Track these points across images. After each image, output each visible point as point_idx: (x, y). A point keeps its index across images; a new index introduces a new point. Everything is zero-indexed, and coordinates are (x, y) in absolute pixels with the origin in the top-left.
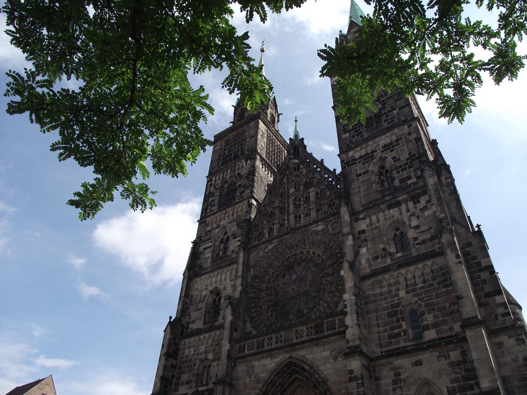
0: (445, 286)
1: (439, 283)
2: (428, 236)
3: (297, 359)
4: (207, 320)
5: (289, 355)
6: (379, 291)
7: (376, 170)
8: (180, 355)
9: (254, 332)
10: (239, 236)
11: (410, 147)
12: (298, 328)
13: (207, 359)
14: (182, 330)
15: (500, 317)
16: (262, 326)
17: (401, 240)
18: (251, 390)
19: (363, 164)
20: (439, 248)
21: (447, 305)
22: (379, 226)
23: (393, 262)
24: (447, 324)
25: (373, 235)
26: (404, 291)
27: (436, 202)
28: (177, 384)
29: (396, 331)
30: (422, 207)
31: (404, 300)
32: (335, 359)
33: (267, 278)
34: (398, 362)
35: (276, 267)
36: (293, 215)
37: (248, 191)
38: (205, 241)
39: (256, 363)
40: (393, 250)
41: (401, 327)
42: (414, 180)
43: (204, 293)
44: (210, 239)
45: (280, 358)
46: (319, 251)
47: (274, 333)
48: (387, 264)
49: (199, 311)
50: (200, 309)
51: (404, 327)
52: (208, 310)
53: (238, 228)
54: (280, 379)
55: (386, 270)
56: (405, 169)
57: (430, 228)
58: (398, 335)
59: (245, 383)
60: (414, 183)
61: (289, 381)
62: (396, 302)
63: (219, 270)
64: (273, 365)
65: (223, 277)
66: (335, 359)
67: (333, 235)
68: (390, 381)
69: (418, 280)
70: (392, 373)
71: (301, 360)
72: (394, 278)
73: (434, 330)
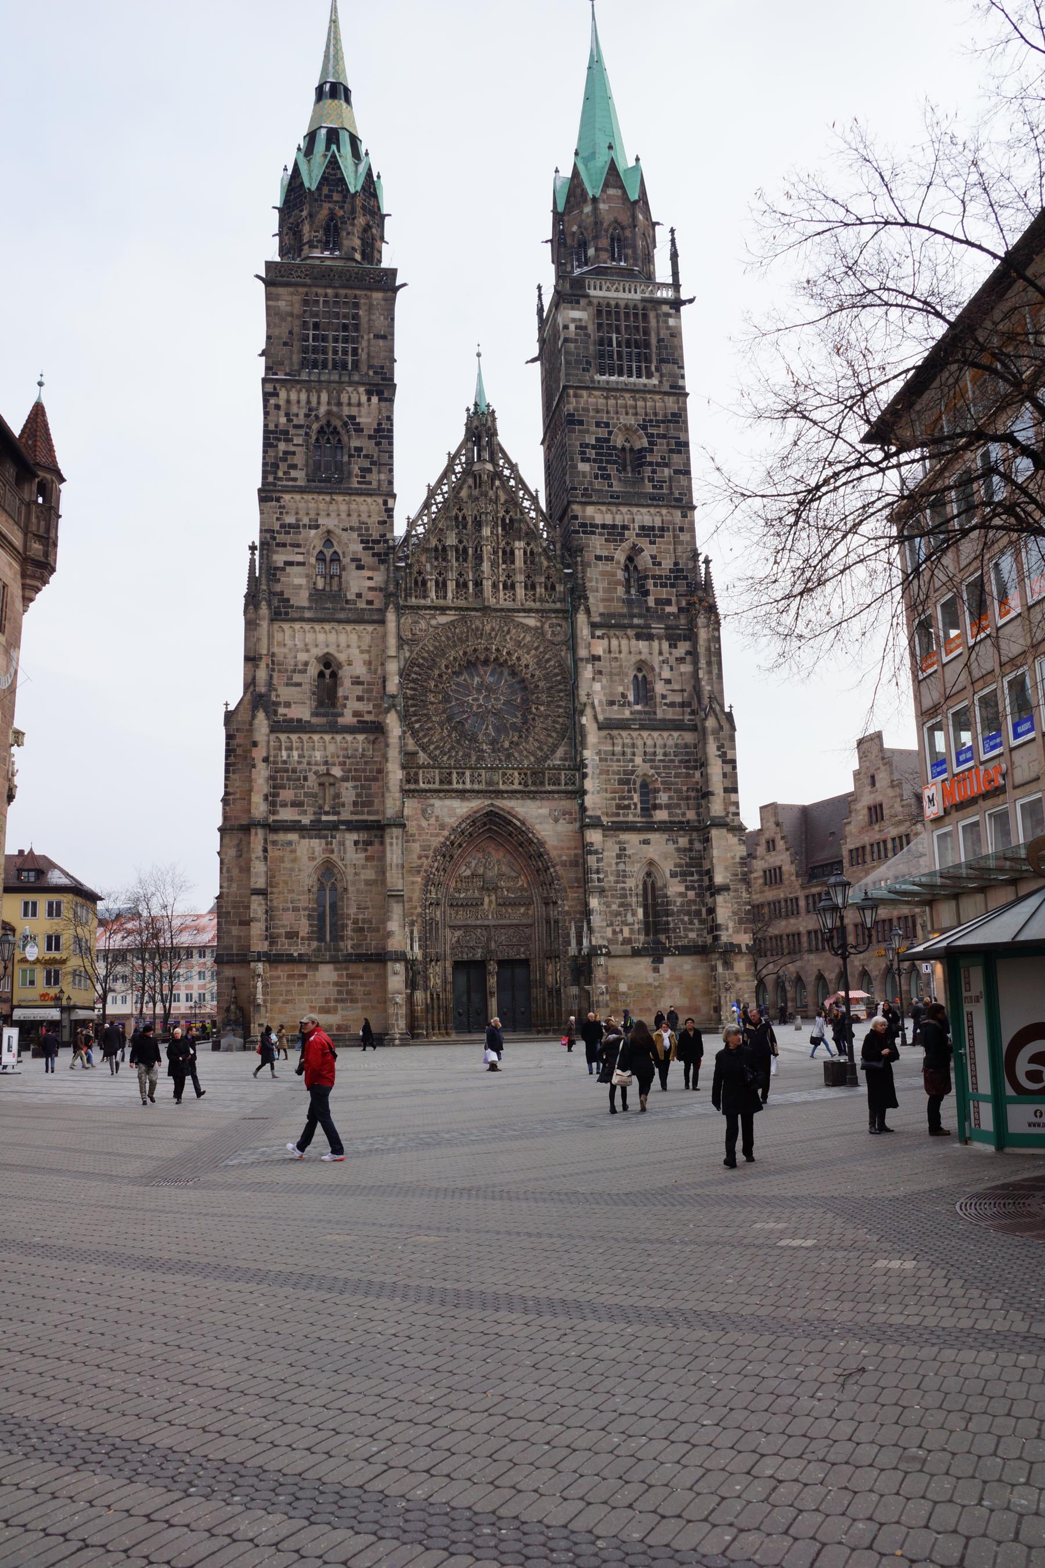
0: (686, 768)
1: (680, 761)
2: (678, 699)
5: (489, 802)
7: (622, 559)
9: (421, 754)
13: (328, 774)
16: (432, 747)
17: (643, 688)
19: (607, 540)
21: (685, 788)
29: (626, 802)
32: (556, 821)
33: (437, 672)
34: (625, 837)
36: (490, 583)
37: (383, 477)
38: (284, 545)
39: (437, 803)
40: (631, 698)
43: (302, 657)
44: (298, 546)
45: (475, 804)
46: (528, 659)
49: (298, 689)
50: (299, 685)
55: (623, 725)
57: (682, 691)
58: (628, 807)
60: (673, 614)
63: (335, 625)
66: (556, 821)
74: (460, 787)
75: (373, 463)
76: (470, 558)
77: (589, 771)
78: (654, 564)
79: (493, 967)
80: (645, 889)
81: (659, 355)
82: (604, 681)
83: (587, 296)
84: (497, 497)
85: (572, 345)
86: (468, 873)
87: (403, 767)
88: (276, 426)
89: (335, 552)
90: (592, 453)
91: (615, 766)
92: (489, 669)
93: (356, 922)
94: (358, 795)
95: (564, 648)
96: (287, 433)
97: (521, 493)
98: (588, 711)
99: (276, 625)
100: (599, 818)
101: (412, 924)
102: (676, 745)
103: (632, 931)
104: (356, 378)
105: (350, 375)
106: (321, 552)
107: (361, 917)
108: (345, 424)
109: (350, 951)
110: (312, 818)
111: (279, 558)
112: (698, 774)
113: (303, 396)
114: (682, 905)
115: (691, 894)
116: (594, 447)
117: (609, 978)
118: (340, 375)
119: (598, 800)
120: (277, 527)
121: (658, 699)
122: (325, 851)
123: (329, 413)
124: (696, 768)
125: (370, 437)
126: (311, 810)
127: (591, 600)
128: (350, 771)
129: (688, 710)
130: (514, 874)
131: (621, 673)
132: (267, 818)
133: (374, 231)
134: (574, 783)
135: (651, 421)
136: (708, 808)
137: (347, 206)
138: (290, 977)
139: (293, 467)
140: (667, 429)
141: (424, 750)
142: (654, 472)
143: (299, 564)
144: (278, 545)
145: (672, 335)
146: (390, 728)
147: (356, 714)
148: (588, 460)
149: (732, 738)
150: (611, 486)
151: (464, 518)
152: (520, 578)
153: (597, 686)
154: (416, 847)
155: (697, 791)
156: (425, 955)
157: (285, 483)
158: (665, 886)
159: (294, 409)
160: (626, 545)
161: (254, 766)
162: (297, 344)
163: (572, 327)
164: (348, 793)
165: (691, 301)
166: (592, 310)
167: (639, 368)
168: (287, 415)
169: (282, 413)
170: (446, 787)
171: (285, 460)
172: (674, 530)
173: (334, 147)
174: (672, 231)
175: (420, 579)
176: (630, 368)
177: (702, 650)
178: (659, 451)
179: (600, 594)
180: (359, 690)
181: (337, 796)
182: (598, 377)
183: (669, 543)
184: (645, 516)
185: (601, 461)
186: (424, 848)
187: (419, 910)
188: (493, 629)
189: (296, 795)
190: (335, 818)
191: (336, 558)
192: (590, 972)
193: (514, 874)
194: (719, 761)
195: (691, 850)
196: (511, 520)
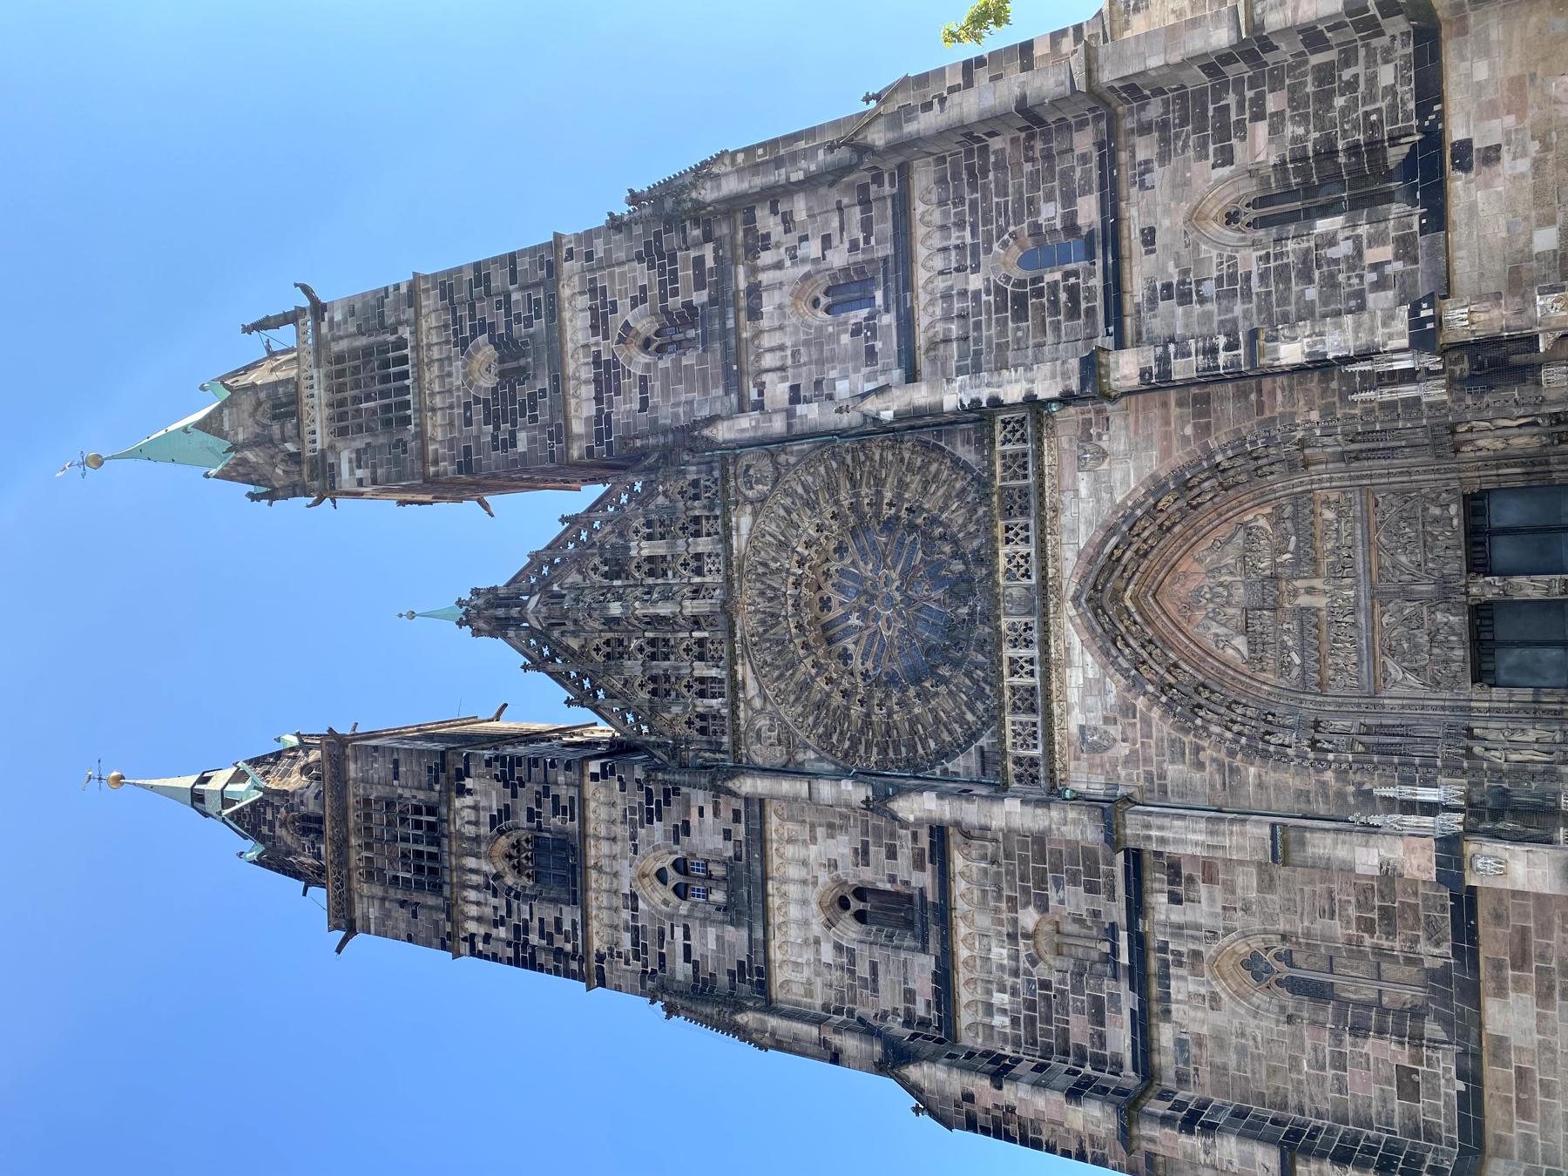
0: (985, 174)
1: (974, 189)
2: (856, 214)
3: (1084, 577)
4: (913, 944)
5: (1069, 604)
6: (955, 345)
7: (644, 359)
8: (1008, 1051)
9: (984, 741)
11: (622, 255)
12: (1002, 569)
14: (926, 1037)
16: (970, 717)
17: (845, 291)
20: (892, 185)
21: (1028, 167)
22: (794, 345)
23: (893, 307)
24: (1073, 168)
25: (810, 362)
26: (972, 277)
28: (1099, 1062)
29: (1063, 296)
30: (781, 228)
32: (1103, 455)
33: (837, 699)
35: (813, 671)
36: (687, 603)
37: (561, 779)
38: (662, 957)
39: (1075, 720)
41: (1056, 283)
42: (708, 251)
43: (828, 953)
44: (662, 933)
47: (1001, 649)
48: (894, 325)
49: (881, 969)
50: (874, 967)
51: (1058, 276)
52: (882, 939)
53: (660, 819)
54: (1132, 642)
56: (674, 272)
57: (840, 209)
58: (1073, 292)
59: (1130, 760)
60: (716, 251)
61: (1138, 619)
62: (992, 298)
64: (1089, 659)
65: (794, 872)
66: (1103, 455)
67: (776, 481)
68: (1180, 310)
69: (954, 241)
70: (1162, 305)
71: (1089, 563)
72: (932, 303)
73: (1079, 200)
74: (1037, 668)
75: (546, 789)
76: (661, 635)
77: (984, 395)
78: (644, 300)
79: (1487, 588)
80: (1262, 223)
82: (833, 374)
84: (573, 587)
85: (379, 471)
86: (1240, 642)
87: (1000, 790)
88: (509, 944)
89: (675, 865)
92: (836, 598)
93: (1367, 926)
94: (1074, 881)
95: (782, 458)
96: (517, 927)
98: (870, 406)
99: (777, 993)
101: (1366, 796)
102: (942, 203)
103: (1377, 240)
106: (676, 890)
107: (1352, 912)
108: (501, 832)
109: (1446, 949)
110: (1124, 985)
111: (681, 970)
112: (996, 143)
113: (472, 895)
114: (1305, 117)
116: (497, 428)
117: (1519, 279)
119: (1046, 368)
120: (637, 966)
121: (860, 257)
122: (1196, 972)
123: (489, 857)
124: (984, 150)
125: (514, 795)
126: (1107, 984)
127: (705, 412)
128: (1026, 890)
129: (873, 188)
130: (1241, 534)
131: (818, 340)
134: (1021, 422)
137: (277, 801)
138: (1525, 1111)
139: (558, 922)
141: (973, 736)
142: (518, 318)
143: (687, 936)
144: (662, 966)
145: (352, 314)
147: (919, 865)
148: (513, 435)
149: (922, 80)
150: (543, 391)
151: (607, 643)
153: (843, 388)
154: (1174, 771)
155: (1031, 137)
156: (1453, 770)
157: (580, 942)
158: (1251, 173)
159: (488, 911)
161: (1011, 1110)
162: (416, 897)
163: (359, 473)
164: (1071, 900)
165: (306, 290)
166: (339, 445)
168: (496, 924)
171: (550, 935)
172: (591, 270)
175: (698, 723)
177: (758, 182)
178: (492, 315)
180: (877, 853)
181: (1079, 920)
182: (411, 427)
183: (612, 276)
184: (576, 326)
185: (513, 411)
186: (1178, 754)
187: (1329, 776)
188: (762, 594)
190: (1123, 935)
191: (681, 866)
192: (1494, 342)
193: (1241, 534)
196: (605, 563)
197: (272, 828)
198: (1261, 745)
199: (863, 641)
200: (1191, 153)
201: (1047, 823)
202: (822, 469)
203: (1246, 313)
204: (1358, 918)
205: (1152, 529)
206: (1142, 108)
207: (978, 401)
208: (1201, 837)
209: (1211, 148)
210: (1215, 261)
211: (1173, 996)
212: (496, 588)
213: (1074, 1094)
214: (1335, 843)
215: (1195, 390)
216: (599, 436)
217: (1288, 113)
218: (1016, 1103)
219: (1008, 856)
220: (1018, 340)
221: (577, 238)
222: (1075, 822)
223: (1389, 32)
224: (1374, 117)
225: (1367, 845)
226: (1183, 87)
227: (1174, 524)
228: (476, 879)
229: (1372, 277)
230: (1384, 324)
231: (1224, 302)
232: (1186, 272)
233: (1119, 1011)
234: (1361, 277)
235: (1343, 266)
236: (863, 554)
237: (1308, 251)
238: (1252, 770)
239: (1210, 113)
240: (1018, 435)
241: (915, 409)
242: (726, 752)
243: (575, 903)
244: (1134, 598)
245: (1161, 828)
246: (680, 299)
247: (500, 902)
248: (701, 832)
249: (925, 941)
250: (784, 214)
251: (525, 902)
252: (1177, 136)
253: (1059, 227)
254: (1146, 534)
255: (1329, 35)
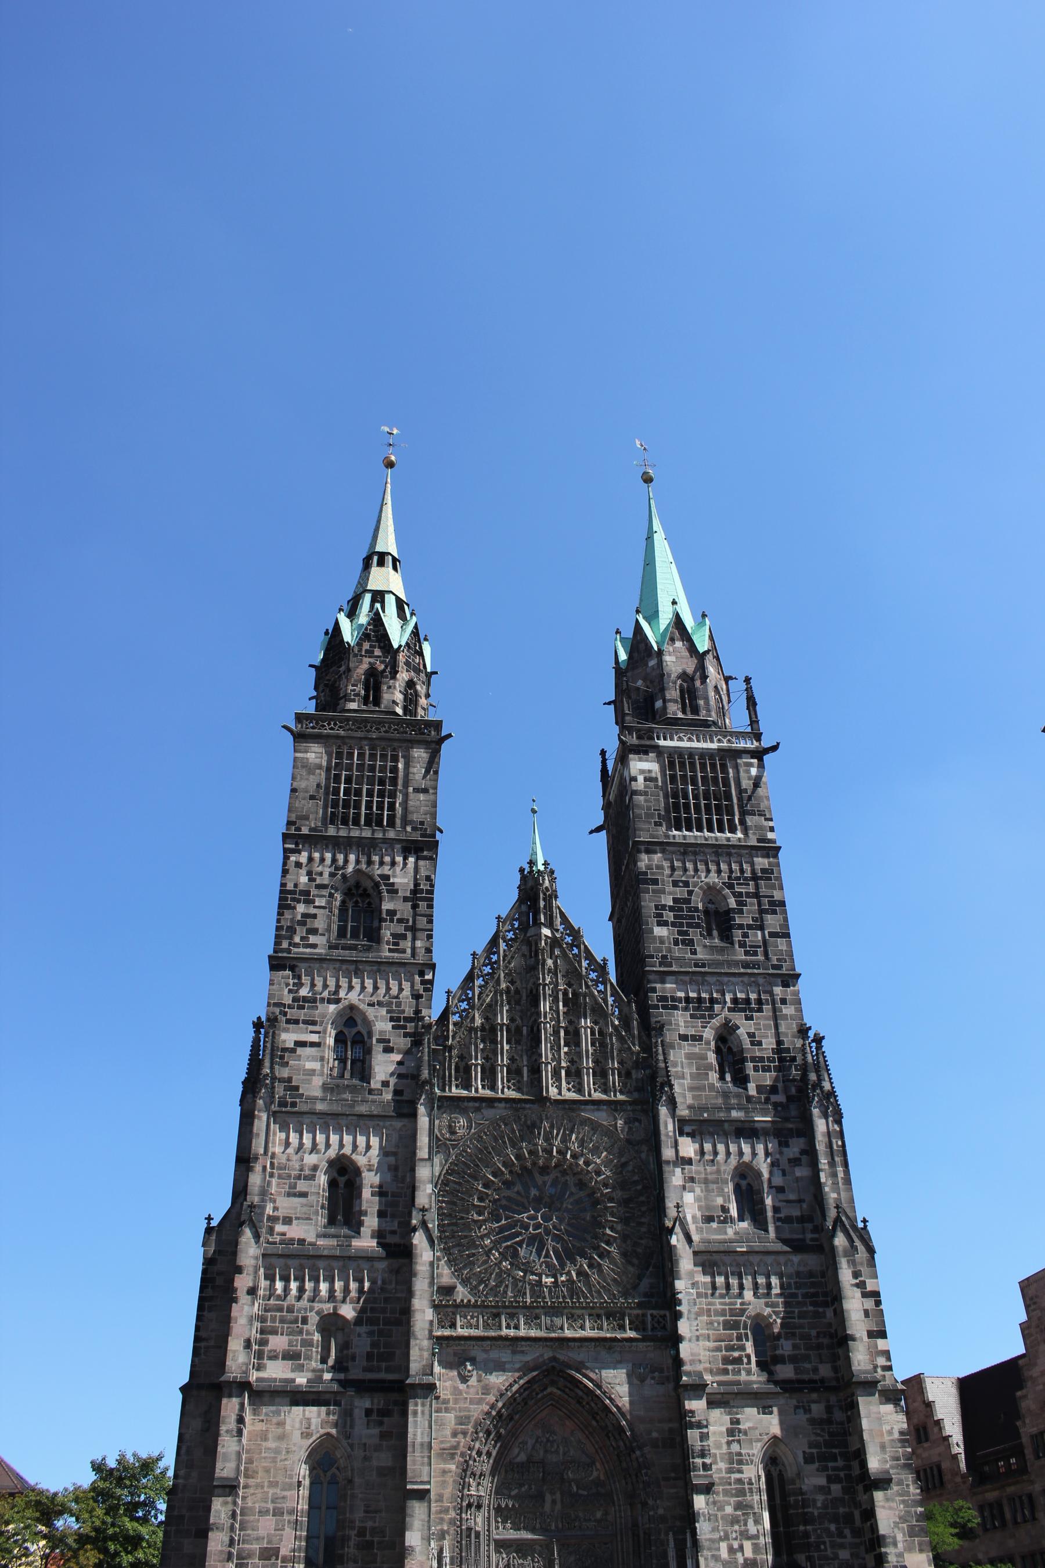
0: (813, 1304)
1: (805, 1296)
2: (796, 1212)
5: (551, 1354)
9: (460, 1288)
10: (399, 1052)
15: (879, 1370)
18: (471, 1403)
19: (692, 1016)
20: (812, 1240)
21: (814, 1333)
25: (706, 1174)
27: (827, 1167)
28: (260, 1355)
29: (736, 1354)
30: (791, 1156)
31: (751, 1307)
38: (296, 1022)
40: (734, 1212)
43: (310, 1159)
44: (314, 1023)
50: (304, 1195)
53: (393, 1027)
57: (800, 1201)
58: (738, 1361)
61: (540, 1396)
62: (738, 1306)
70: (728, 1417)
73: (792, 1366)
74: (512, 1333)
77: (683, 1308)
78: (752, 1043)
81: (741, 806)
82: (698, 1190)
83: (657, 747)
85: (642, 798)
86: (522, 1458)
88: (296, 885)
89: (359, 1033)
90: (669, 916)
91: (718, 1304)
92: (549, 1179)
93: (361, 1533)
94: (373, 1345)
95: (645, 1148)
96: (307, 893)
97: (585, 964)
100: (700, 1375)
101: (442, 1536)
103: (756, 1548)
104: (391, 834)
105: (384, 832)
107: (369, 1524)
111: (288, 1038)
112: (829, 1313)
114: (825, 1506)
115: (836, 1488)
116: (671, 909)
118: (373, 831)
120: (288, 999)
123: (358, 871)
124: (826, 1304)
125: (406, 899)
127: (677, 1089)
132: (246, 1372)
133: (418, 687)
134: (664, 1327)
135: (738, 878)
136: (848, 1359)
139: (314, 931)
140: (757, 887)
141: (465, 1282)
142: (745, 935)
143: (313, 1044)
144: (288, 1021)
146: (417, 1251)
148: (665, 924)
150: (694, 953)
152: (588, 1063)
153: (689, 1198)
155: (831, 1336)
157: (301, 950)
158: (798, 1474)
160: (716, 1022)
161: (235, 1300)
163: (641, 779)
165: (774, 748)
167: (720, 822)
168: (309, 873)
169: (303, 871)
170: (492, 1333)
171: (303, 923)
173: (378, 605)
174: (747, 680)
176: (709, 822)
177: (821, 1146)
178: (749, 912)
179: (687, 1081)
183: (767, 1019)
185: (681, 925)
186: (461, 1421)
187: (452, 1514)
189: (290, 1344)
194: (857, 1293)
195: (829, 1421)
196: (574, 993)
197: (370, 653)
198: (469, 1473)
199: (519, 1198)
200: (813, 1438)
201: (419, 1337)
202: (636, 1178)
203: (721, 1470)
204: (365, 1528)
205: (596, 1408)
206: (841, 1408)
207: (680, 1304)
208: (419, 1439)
209: (814, 1451)
210: (751, 1452)
211: (307, 1408)
212: (556, 897)
213: (248, 1344)
214: (423, 1521)
215: (678, 1439)
216: (663, 999)
217: (830, 1497)
218: (240, 1304)
219: (386, 1300)
220: (711, 1323)
221: (797, 993)
222: (421, 1356)
223: (867, 1557)
224: (822, 1547)
225: (423, 1539)
226: (850, 1435)
227: (597, 1422)
228: (340, 857)
229: (736, 1545)
230: (713, 1556)
231: (727, 1457)
232: (746, 1433)
233: (293, 1371)
234: (736, 1539)
235: (743, 1528)
236: (578, 1202)
237: (752, 1508)
238: (453, 1467)
239: (834, 1451)
240: (656, 1325)
241: (677, 1261)
242: (444, 1090)
243: (330, 947)
244: (551, 1394)
245: (423, 1412)
246: (751, 1072)
247: (325, 879)
248: (386, 1062)
249: (325, 1236)
250: (799, 1160)
251: (328, 902)
252: (823, 1430)
253: (777, 1352)
254: (593, 1405)
255: (869, 1524)
